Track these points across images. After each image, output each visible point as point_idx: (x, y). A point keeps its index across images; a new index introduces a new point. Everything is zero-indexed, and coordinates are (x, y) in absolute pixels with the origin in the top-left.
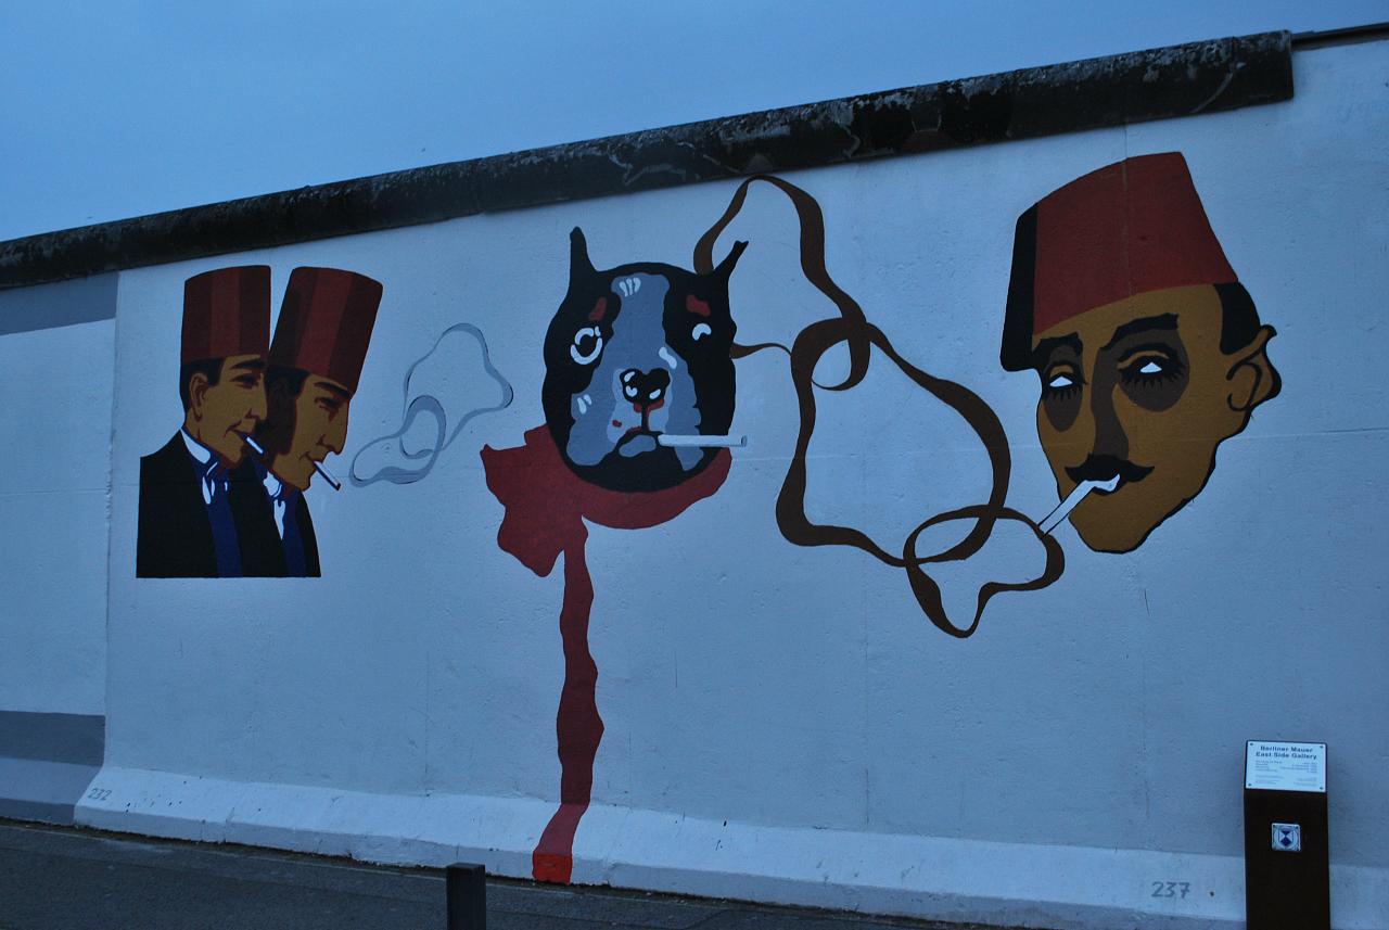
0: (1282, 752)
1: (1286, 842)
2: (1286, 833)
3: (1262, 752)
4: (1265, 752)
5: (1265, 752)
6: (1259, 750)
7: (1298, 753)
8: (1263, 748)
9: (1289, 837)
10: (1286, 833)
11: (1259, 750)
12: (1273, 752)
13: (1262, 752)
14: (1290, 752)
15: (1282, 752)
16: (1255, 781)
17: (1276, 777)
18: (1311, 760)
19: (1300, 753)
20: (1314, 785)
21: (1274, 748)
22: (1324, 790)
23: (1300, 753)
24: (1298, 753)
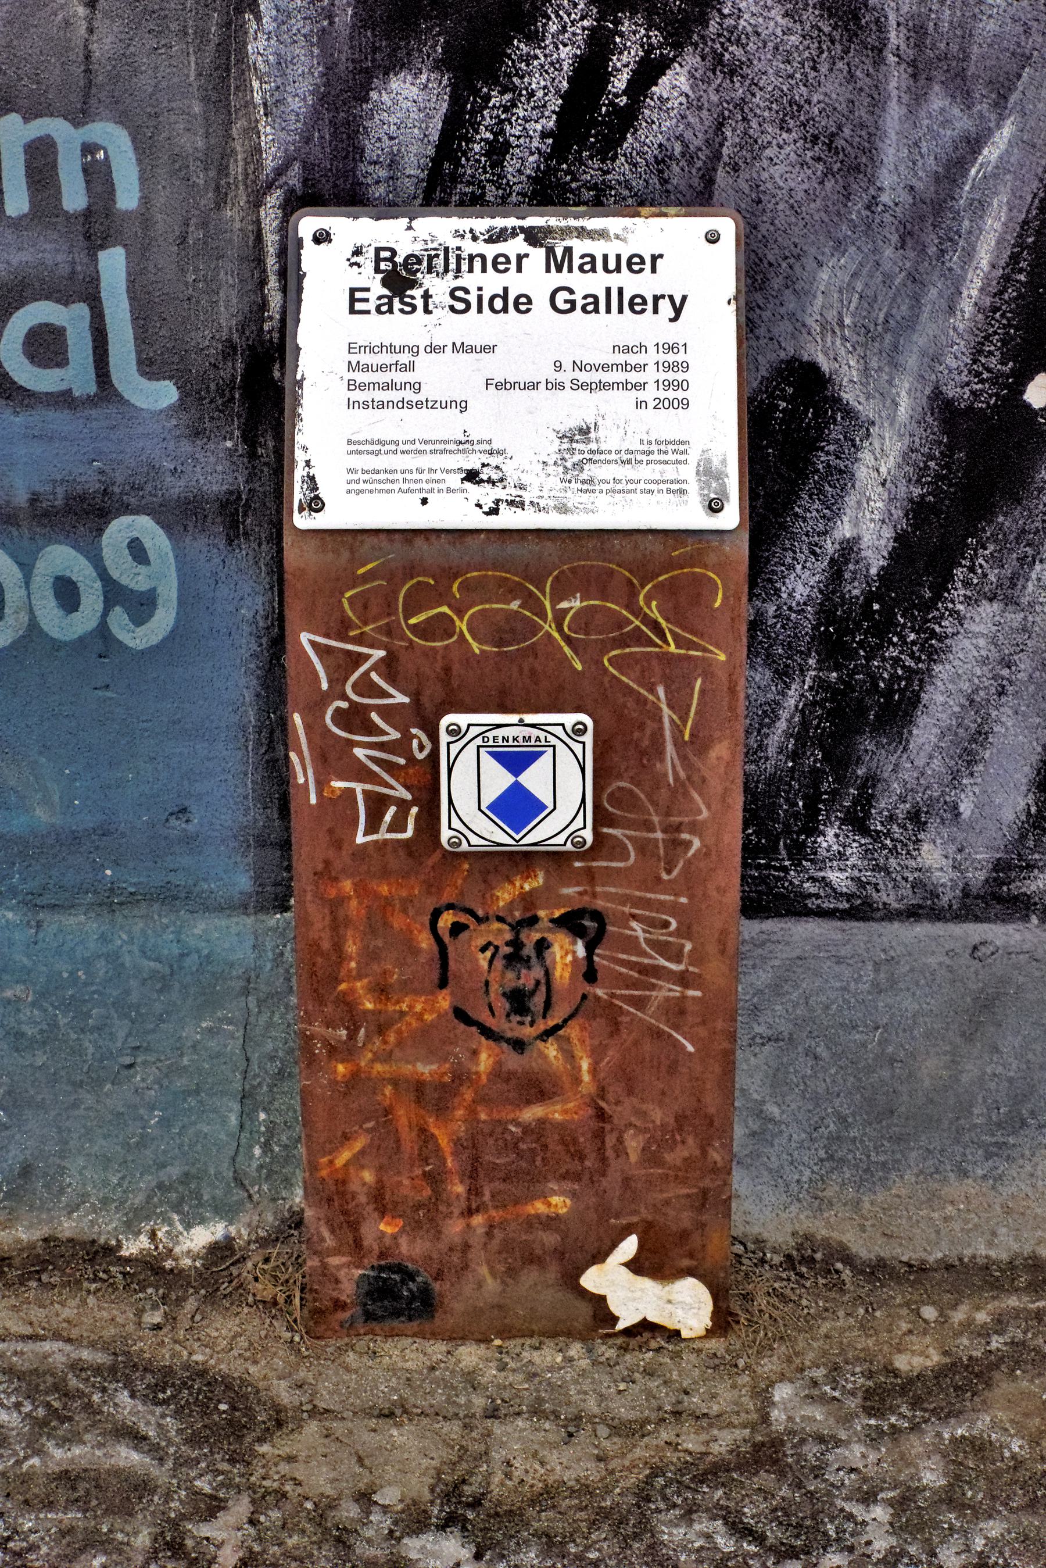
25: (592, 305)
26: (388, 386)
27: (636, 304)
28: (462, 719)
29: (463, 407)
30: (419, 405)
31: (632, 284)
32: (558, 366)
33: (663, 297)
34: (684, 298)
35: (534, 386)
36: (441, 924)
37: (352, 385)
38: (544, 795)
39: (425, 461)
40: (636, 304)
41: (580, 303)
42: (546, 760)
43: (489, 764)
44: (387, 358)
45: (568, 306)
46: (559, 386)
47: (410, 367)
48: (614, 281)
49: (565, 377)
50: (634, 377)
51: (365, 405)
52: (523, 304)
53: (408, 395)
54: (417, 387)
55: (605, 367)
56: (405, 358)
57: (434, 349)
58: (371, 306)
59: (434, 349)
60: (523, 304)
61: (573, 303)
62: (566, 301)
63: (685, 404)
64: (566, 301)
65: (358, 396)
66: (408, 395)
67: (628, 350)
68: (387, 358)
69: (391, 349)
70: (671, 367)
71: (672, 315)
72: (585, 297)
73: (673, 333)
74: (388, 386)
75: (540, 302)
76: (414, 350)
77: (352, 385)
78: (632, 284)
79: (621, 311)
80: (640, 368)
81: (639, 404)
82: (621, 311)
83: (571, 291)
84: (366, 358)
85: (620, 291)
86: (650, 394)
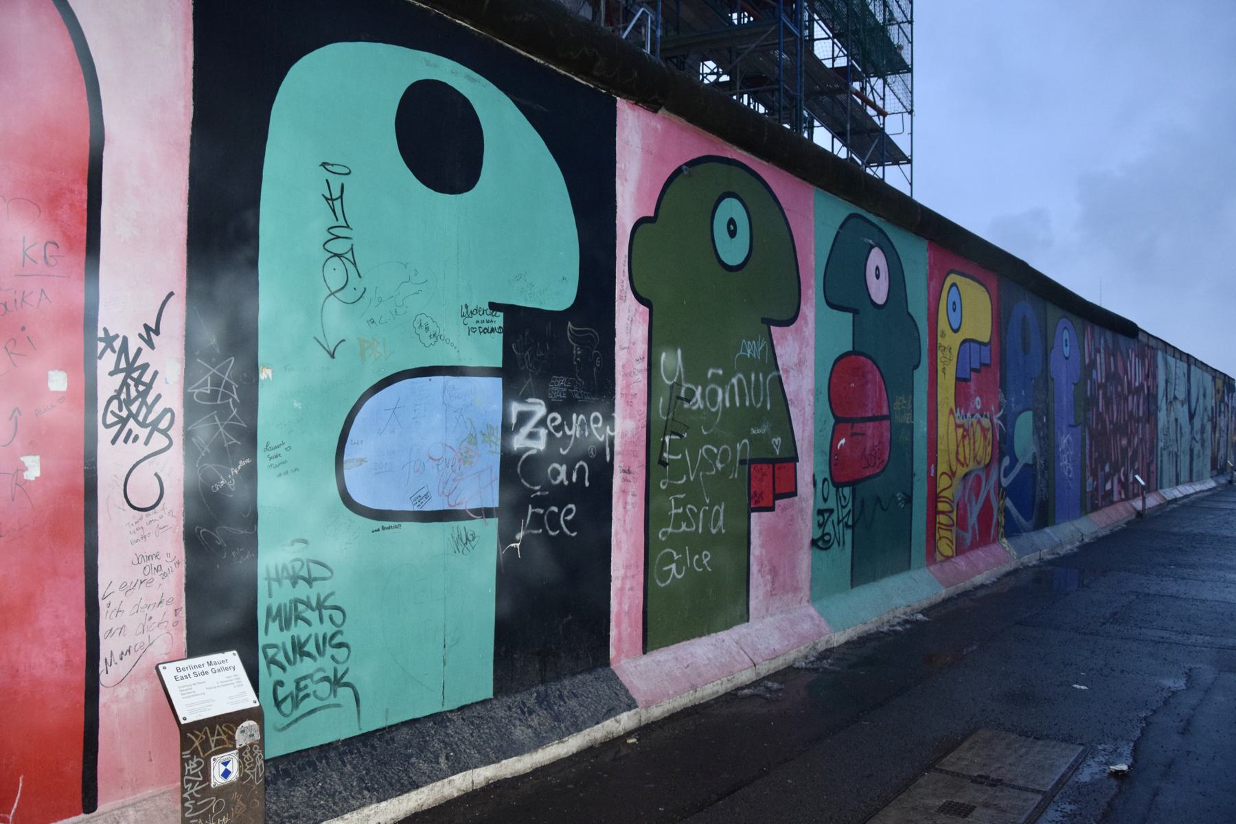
0: (200, 670)
1: (226, 774)
2: (225, 764)
3: (180, 675)
4: (183, 674)
5: (183, 674)
6: (176, 674)
7: (217, 667)
8: (178, 670)
9: (229, 767)
10: (225, 764)
11: (176, 674)
12: (190, 672)
13: (180, 675)
14: (207, 668)
15: (200, 670)
16: (188, 714)
17: (207, 701)
18: (231, 672)
19: (218, 667)
20: (247, 700)
21: (190, 667)
22: (257, 704)
23: (218, 667)
24: (217, 667)
25: (219, 671)
26: (189, 693)
28: (216, 757)
29: (204, 694)
30: (197, 695)
32: (218, 683)
35: (215, 687)
36: (821, 546)
37: (182, 694)
38: (231, 770)
39: (201, 705)
42: (231, 762)
43: (221, 765)
44: (187, 688)
46: (219, 687)
47: (191, 689)
49: (220, 684)
50: (232, 682)
51: (186, 697)
52: (207, 673)
53: (193, 694)
54: (194, 692)
55: (226, 681)
56: (190, 687)
57: (195, 684)
58: (179, 678)
59: (195, 684)
60: (207, 673)
63: (242, 685)
65: (184, 696)
66: (193, 694)
67: (228, 677)
68: (187, 688)
69: (186, 686)
70: (237, 679)
73: (235, 673)
74: (189, 693)
75: (210, 671)
76: (191, 685)
77: (182, 694)
80: (232, 680)
81: (235, 687)
84: (183, 689)
86: (236, 684)
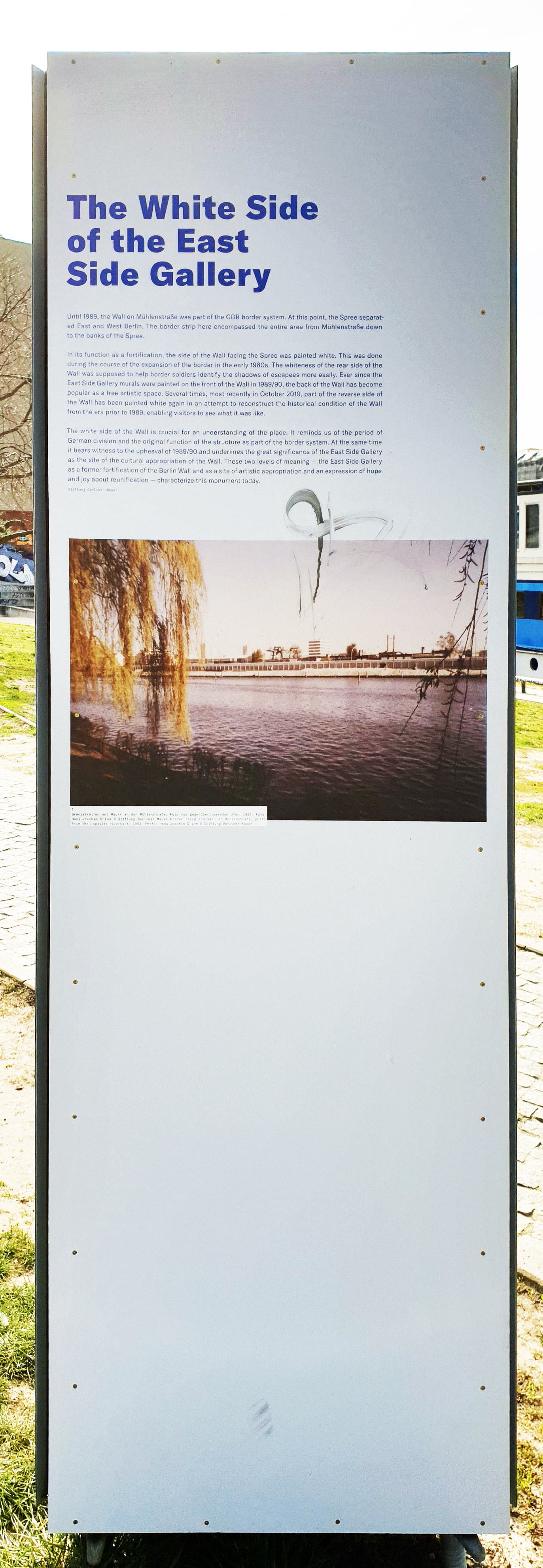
27: (226, 277)
31: (222, 261)
33: (248, 272)
34: (267, 272)
40: (226, 277)
41: (175, 277)
45: (164, 279)
48: (207, 258)
61: (169, 276)
62: (164, 274)
64: (164, 274)
71: (257, 286)
72: (180, 272)
78: (222, 261)
79: (211, 283)
82: (211, 283)
83: (168, 266)
85: (212, 265)
